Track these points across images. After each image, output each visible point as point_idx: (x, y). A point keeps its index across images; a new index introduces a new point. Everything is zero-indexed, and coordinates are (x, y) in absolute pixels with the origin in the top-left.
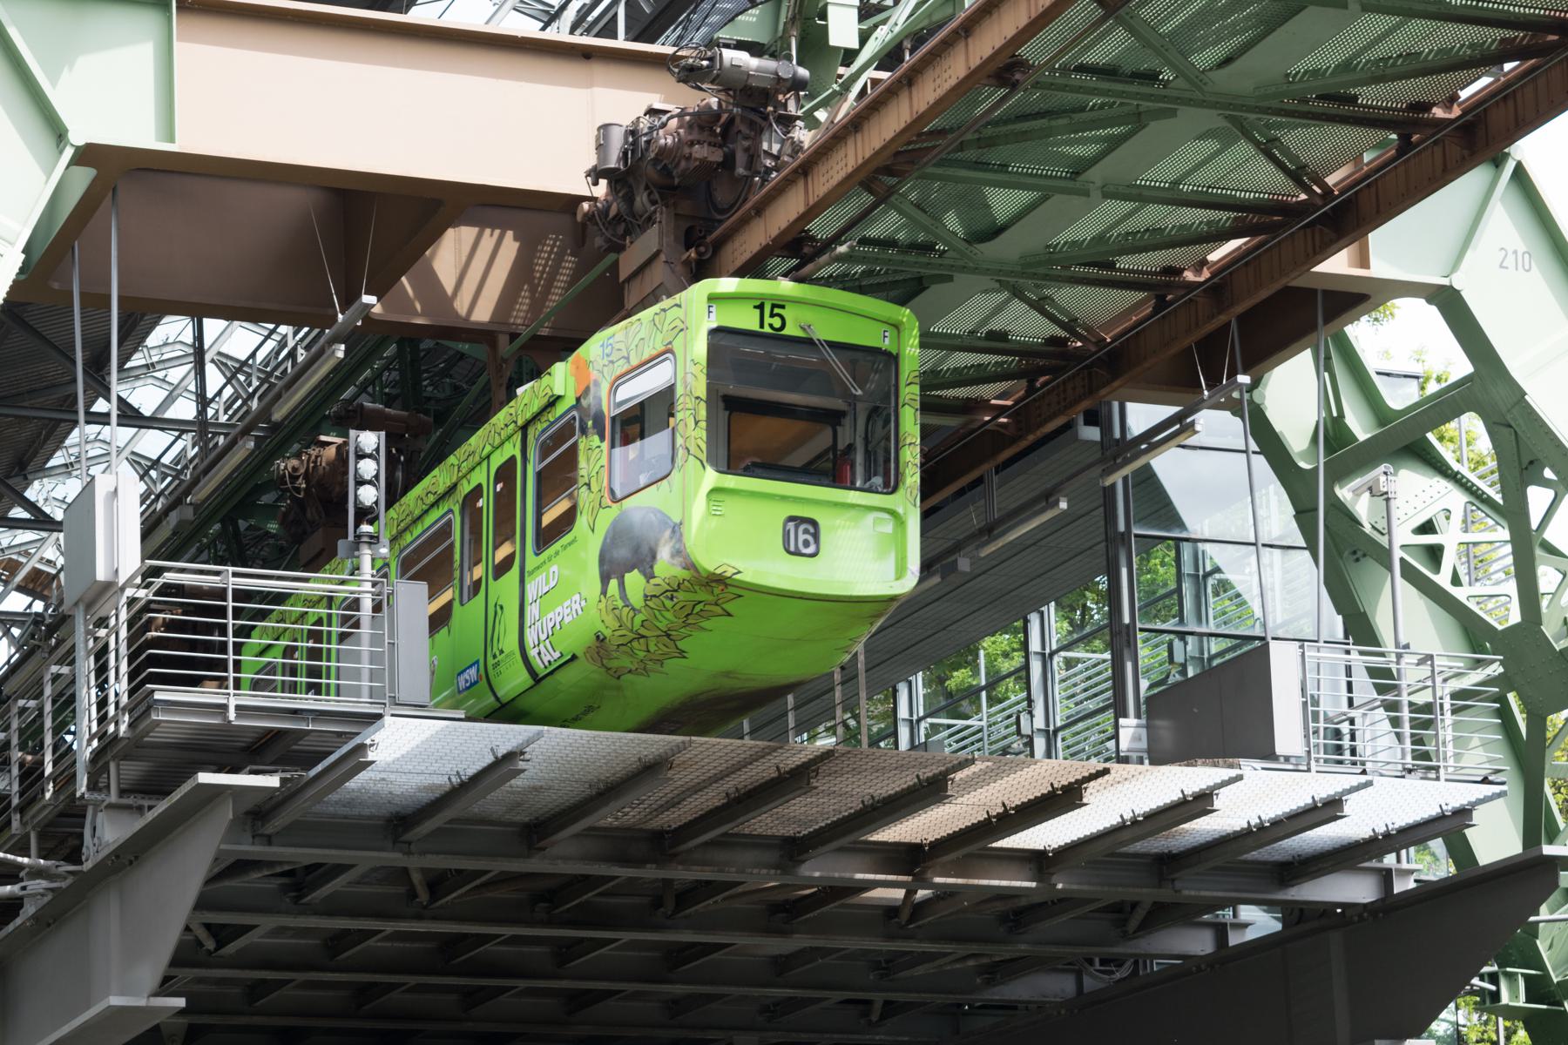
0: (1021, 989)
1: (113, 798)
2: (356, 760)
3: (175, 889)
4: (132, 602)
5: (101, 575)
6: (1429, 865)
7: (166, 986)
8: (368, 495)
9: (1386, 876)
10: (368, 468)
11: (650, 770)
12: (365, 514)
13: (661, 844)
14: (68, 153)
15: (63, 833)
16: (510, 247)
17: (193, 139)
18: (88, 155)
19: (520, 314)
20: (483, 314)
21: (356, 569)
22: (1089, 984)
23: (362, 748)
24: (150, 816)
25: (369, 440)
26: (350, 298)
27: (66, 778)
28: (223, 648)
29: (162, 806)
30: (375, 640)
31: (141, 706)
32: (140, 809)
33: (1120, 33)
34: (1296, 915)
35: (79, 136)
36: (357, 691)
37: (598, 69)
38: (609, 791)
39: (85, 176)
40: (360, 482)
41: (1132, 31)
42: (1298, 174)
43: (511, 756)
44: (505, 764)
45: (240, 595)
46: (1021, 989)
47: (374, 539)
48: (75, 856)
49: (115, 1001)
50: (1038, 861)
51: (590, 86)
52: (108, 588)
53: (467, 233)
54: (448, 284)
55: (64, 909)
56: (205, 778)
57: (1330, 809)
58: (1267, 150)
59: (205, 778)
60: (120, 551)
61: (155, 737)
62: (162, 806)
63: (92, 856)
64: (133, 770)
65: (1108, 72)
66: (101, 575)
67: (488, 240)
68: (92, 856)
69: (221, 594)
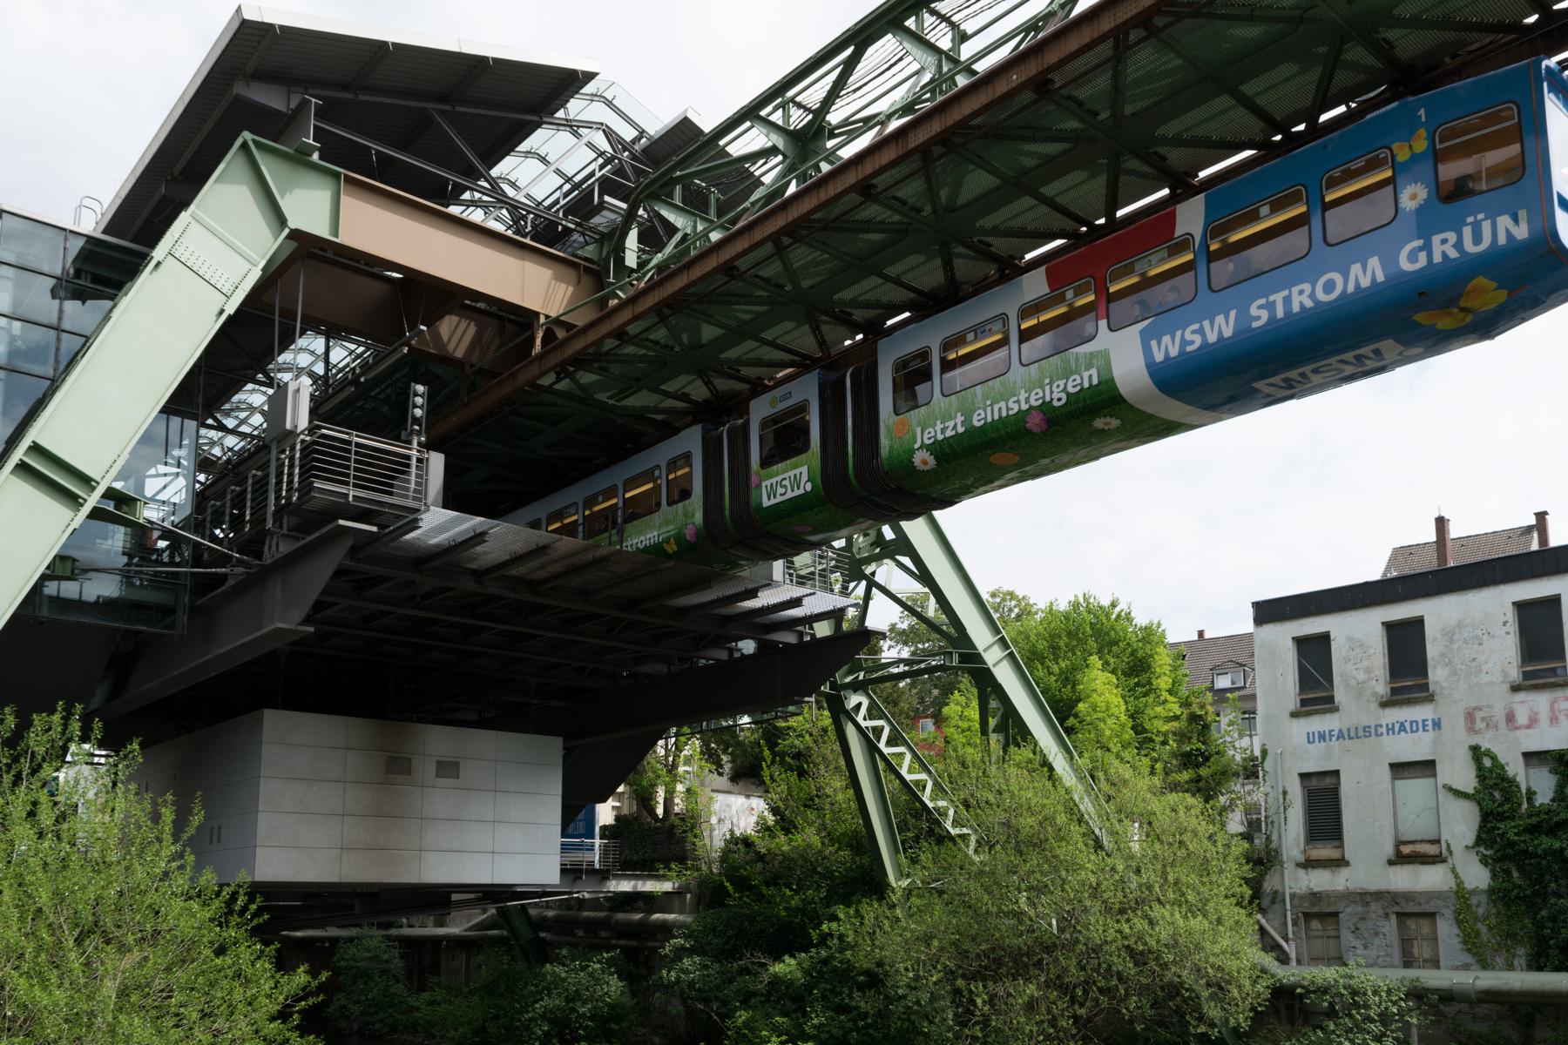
0: (647, 668)
1: (285, 531)
2: (413, 525)
3: (317, 575)
4: (303, 441)
5: (288, 426)
6: (823, 629)
7: (307, 620)
8: (418, 412)
9: (801, 634)
10: (419, 401)
11: (541, 550)
12: (416, 421)
13: (532, 585)
14: (286, 231)
15: (252, 545)
16: (472, 329)
17: (345, 239)
18: (296, 235)
19: (475, 358)
20: (459, 354)
21: (410, 442)
22: (673, 669)
23: (416, 520)
24: (301, 543)
25: (420, 388)
26: (413, 327)
27: (259, 520)
28: (348, 467)
29: (309, 539)
30: (418, 476)
31: (306, 488)
32: (298, 539)
33: (778, 263)
34: (763, 645)
35: (293, 223)
36: (406, 497)
37: (527, 254)
38: (517, 559)
39: (293, 245)
40: (415, 406)
41: (784, 263)
42: (822, 343)
43: (483, 534)
44: (478, 537)
45: (358, 445)
46: (647, 668)
47: (419, 433)
48: (259, 556)
49: (280, 625)
50: (682, 611)
51: (523, 259)
52: (292, 434)
53: (455, 319)
54: (445, 339)
55: (255, 581)
56: (341, 522)
57: (796, 602)
58: (816, 330)
59: (341, 522)
60: (299, 416)
61: (310, 506)
62: (309, 539)
63: (268, 559)
64: (295, 520)
65: (767, 280)
66: (288, 426)
67: (464, 324)
68: (268, 559)
69: (349, 443)
